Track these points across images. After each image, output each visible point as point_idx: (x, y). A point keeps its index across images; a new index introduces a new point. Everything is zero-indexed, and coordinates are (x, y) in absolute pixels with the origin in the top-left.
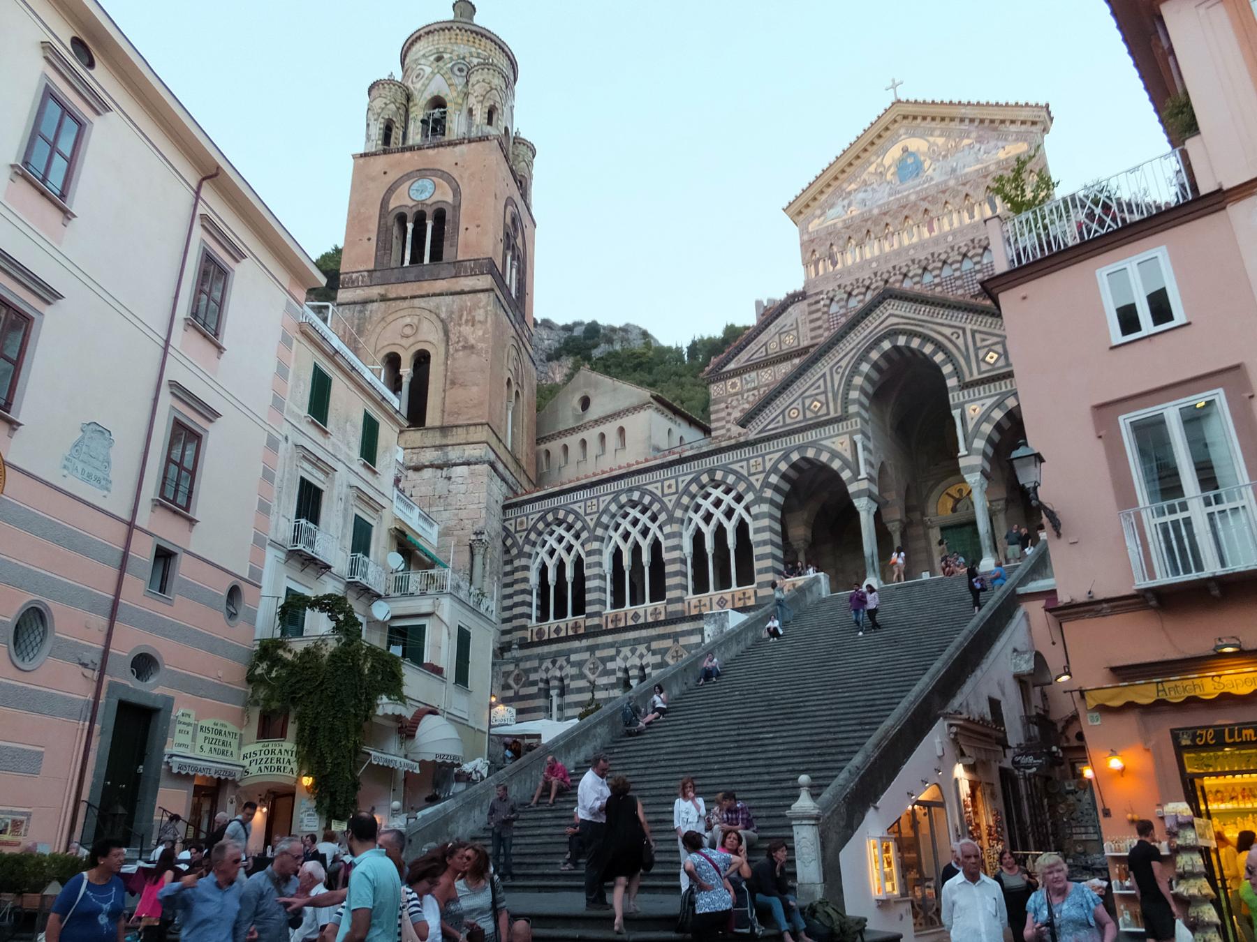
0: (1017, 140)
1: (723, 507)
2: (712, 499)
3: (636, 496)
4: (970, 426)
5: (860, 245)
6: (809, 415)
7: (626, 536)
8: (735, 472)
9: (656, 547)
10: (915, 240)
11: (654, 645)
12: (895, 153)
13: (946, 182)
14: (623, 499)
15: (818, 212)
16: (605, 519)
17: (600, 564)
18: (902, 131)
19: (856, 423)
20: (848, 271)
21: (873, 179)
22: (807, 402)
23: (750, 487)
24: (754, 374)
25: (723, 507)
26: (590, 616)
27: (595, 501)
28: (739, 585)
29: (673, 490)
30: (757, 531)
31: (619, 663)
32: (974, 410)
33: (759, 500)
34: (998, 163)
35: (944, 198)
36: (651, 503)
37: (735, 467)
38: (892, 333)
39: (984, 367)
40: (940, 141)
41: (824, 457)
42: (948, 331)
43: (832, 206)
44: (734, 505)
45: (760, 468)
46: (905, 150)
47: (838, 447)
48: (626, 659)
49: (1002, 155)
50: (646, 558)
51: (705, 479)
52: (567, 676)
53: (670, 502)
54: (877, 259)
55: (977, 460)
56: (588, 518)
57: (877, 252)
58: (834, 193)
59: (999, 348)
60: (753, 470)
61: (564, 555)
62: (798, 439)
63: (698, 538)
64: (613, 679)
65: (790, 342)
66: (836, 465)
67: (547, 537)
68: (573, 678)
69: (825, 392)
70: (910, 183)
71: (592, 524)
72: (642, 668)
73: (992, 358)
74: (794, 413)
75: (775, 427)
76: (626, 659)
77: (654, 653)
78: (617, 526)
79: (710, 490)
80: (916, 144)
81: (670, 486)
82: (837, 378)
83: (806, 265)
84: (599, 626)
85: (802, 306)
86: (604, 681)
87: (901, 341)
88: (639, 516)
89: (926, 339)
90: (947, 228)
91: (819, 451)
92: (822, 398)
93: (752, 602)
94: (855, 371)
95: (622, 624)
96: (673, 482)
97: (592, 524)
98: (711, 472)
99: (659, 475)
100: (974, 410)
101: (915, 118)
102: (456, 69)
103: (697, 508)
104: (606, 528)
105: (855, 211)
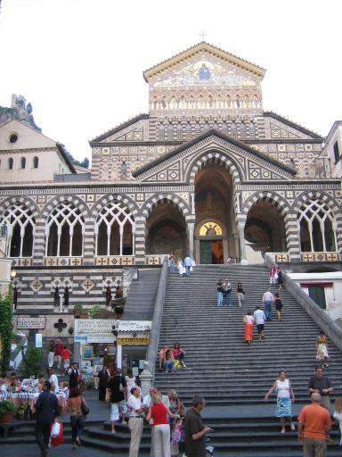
0: (251, 80)
1: (119, 214)
2: (113, 209)
3: (70, 199)
4: (243, 202)
5: (178, 102)
6: (170, 178)
7: (60, 219)
8: (128, 198)
9: (78, 227)
10: (203, 108)
11: (75, 278)
12: (198, 65)
13: (220, 86)
14: (62, 199)
15: (159, 79)
16: (50, 208)
17: (43, 231)
18: (203, 56)
19: (192, 188)
21: (187, 73)
22: (170, 172)
23: (136, 207)
24: (117, 148)
25: (119, 214)
26: (35, 258)
27: (44, 197)
28: (123, 254)
29: (92, 200)
30: (138, 229)
31: (53, 284)
32: (246, 195)
33: (140, 214)
34: (243, 86)
35: (220, 93)
36: (78, 205)
37: (129, 195)
38: (214, 151)
39: (252, 177)
40: (220, 67)
41: (176, 201)
42: (238, 157)
43: (166, 78)
44: (125, 214)
45: (142, 199)
46: (204, 65)
47: (183, 197)
48: (57, 283)
49: (245, 84)
50: (71, 232)
51: (111, 198)
52: (19, 288)
53: (90, 206)
54: (186, 111)
55: (245, 217)
56: (39, 205)
57: (185, 107)
58: (167, 73)
59: (258, 171)
60: (138, 199)
62: (163, 189)
63: (103, 227)
64: (48, 293)
65: (138, 137)
66: (181, 205)
67: (10, 211)
68: (23, 289)
69: (179, 170)
70: (204, 81)
71: (41, 209)
73: (255, 174)
74: (162, 176)
75: (152, 180)
76: (57, 283)
77: (75, 282)
78: (55, 213)
79: (112, 204)
80: (208, 64)
81: (91, 198)
82: (185, 165)
83: (150, 103)
84: (40, 264)
85: (147, 121)
86: (43, 293)
87: (217, 156)
88: (69, 209)
89: (228, 158)
90: (218, 107)
91: (174, 197)
92: (177, 172)
93: (130, 264)
94: (195, 164)
95: (55, 265)
96: (93, 196)
97: (41, 209)
98: (115, 195)
99: (85, 190)
100: (246, 195)
101: (210, 53)
103: (104, 212)
104: (49, 212)
105: (178, 84)
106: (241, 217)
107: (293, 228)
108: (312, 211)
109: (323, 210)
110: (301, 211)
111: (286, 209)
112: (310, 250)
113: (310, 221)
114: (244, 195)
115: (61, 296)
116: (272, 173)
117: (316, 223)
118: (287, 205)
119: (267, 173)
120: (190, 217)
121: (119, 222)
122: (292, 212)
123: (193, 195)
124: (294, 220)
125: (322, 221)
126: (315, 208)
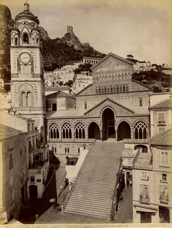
2: (79, 125)
14: (65, 122)
18: (111, 58)
19: (101, 118)
20: (101, 83)
23: (85, 125)
30: (86, 131)
33: (87, 127)
55: (117, 128)
61: (55, 128)
66: (98, 124)
72: (68, 148)
87: (109, 107)
92: (97, 113)
94: (102, 110)
102: (29, 26)
106: (116, 128)
107: (133, 131)
108: (139, 125)
109: (144, 125)
110: (136, 126)
111: (130, 125)
112: (138, 139)
113: (138, 129)
114: (117, 121)
115: (67, 150)
116: (126, 113)
117: (141, 129)
118: (131, 124)
119: (125, 113)
120: (101, 128)
121: (81, 129)
122: (132, 126)
123: (101, 120)
124: (133, 129)
125: (143, 129)
126: (140, 124)
